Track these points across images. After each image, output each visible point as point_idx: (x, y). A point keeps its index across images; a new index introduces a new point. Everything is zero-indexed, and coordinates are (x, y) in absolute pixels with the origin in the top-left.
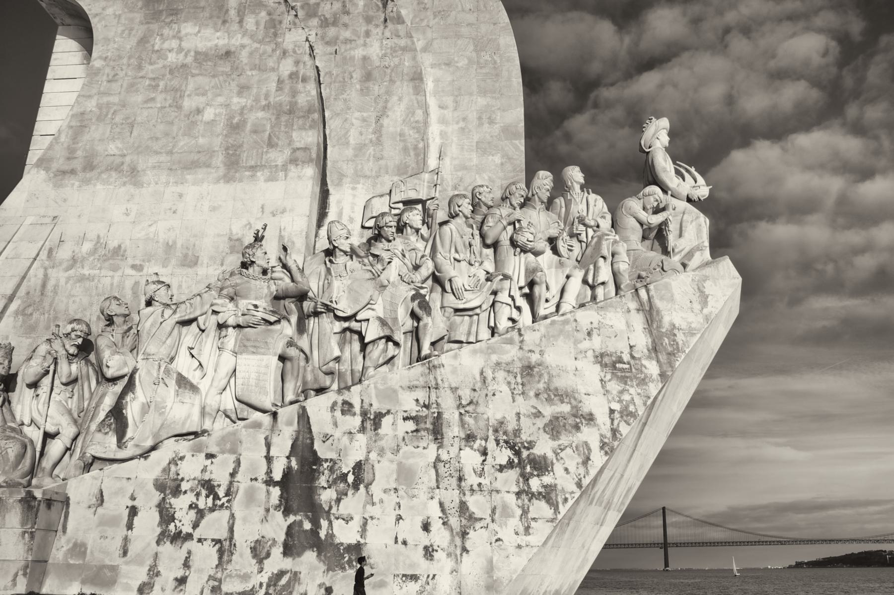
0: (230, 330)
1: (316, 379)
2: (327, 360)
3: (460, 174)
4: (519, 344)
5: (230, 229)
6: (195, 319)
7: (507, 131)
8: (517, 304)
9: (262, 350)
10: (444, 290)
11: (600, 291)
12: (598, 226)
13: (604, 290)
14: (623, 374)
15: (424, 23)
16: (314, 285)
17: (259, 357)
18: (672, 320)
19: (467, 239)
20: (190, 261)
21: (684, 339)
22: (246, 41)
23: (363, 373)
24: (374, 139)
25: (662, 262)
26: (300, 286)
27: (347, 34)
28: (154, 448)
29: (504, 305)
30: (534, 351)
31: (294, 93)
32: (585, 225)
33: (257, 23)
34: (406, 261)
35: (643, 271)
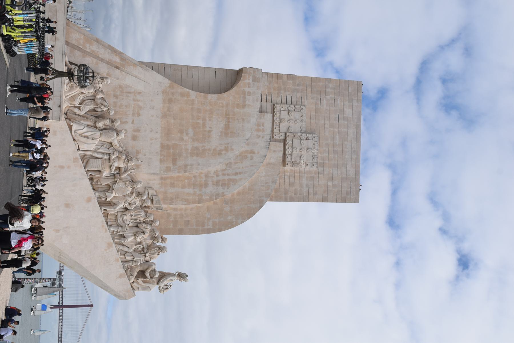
0: (109, 157)
1: (96, 178)
2: (101, 182)
6: (112, 146)
12: (146, 257)
13: (124, 258)
17: (101, 165)
19: (139, 219)
20: (134, 138)
23: (98, 191)
25: (133, 276)
26: (122, 174)
28: (74, 140)
33: (221, 151)
34: (131, 202)
35: (130, 270)
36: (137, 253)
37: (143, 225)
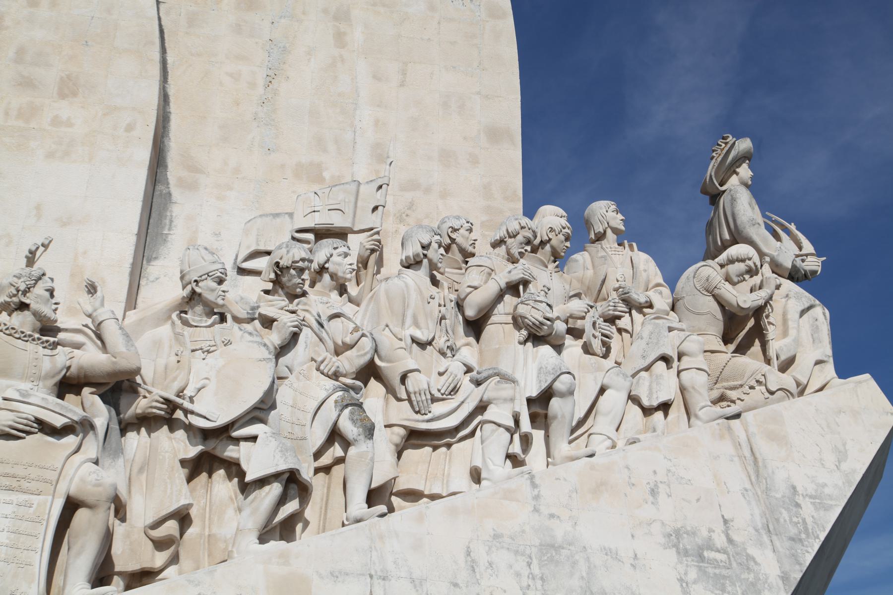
3: (409, 196)
7: (495, 135)
12: (650, 306)
13: (666, 415)
14: (717, 571)
21: (815, 515)
29: (502, 429)
30: (558, 517)
34: (324, 335)
36: (638, 347)
37: (476, 288)
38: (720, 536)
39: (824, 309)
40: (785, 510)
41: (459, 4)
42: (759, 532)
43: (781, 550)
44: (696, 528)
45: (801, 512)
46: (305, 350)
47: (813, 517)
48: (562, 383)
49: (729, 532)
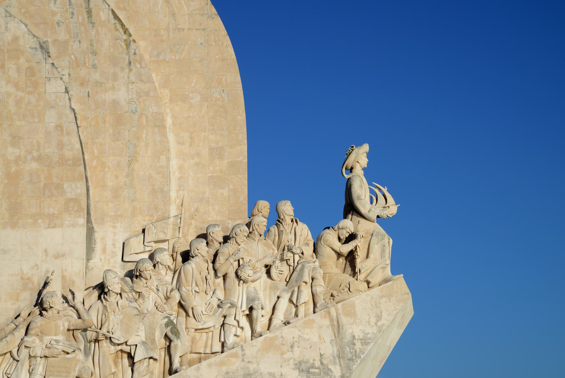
0: (39, 359)
4: (242, 358)
5: (21, 270)
8: (241, 325)
9: (64, 374)
10: (187, 315)
11: (302, 310)
12: (302, 253)
13: (305, 307)
15: (161, 58)
16: (93, 318)
18: (352, 332)
21: (361, 348)
22: (11, 89)
24: (128, 182)
27: (97, 76)
30: (252, 362)
31: (61, 146)
32: (292, 252)
33: (18, 70)
38: (318, 362)
39: (389, 240)
40: (348, 347)
41: (217, 95)
42: (335, 359)
43: (343, 365)
44: (308, 360)
45: (355, 347)
46: (152, 302)
47: (360, 349)
48: (255, 305)
49: (322, 360)
